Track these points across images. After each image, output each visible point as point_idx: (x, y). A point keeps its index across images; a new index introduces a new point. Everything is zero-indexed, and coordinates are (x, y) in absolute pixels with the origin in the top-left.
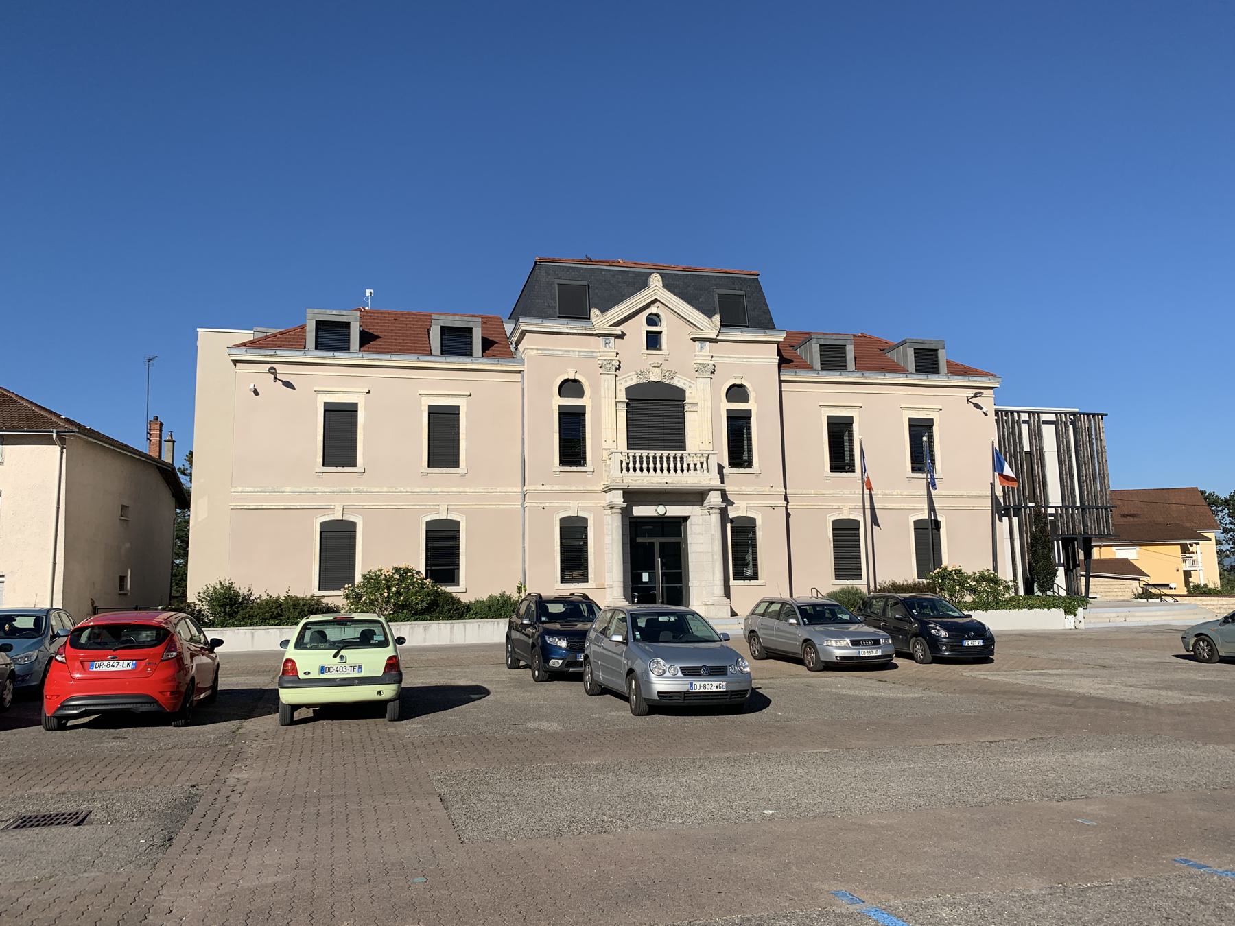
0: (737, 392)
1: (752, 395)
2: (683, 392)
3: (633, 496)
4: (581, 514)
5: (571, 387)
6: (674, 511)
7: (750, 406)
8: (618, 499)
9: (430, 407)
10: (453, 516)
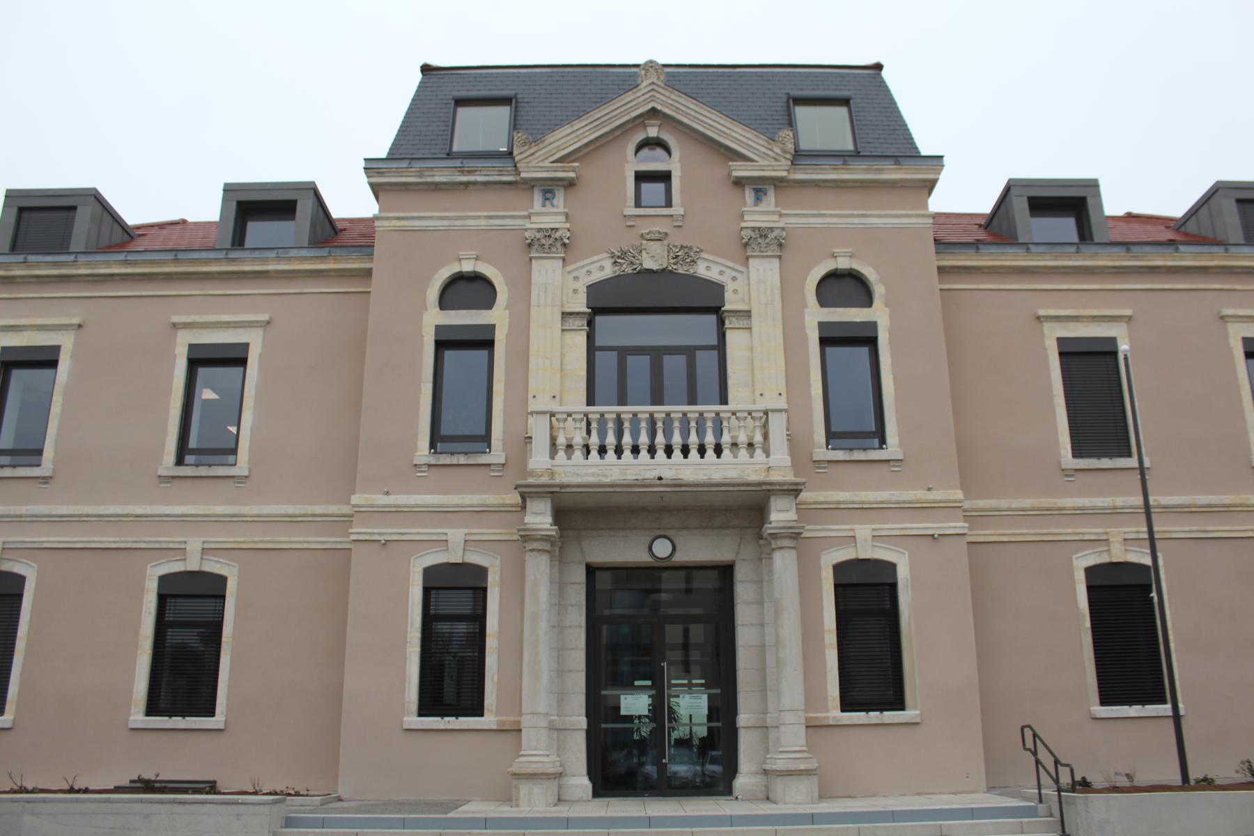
0: (844, 285)
1: (879, 290)
2: (719, 289)
3: (577, 513)
4: (474, 558)
5: (468, 288)
6: (698, 549)
7: (878, 314)
8: (540, 518)
9: (191, 346)
10: (213, 566)
